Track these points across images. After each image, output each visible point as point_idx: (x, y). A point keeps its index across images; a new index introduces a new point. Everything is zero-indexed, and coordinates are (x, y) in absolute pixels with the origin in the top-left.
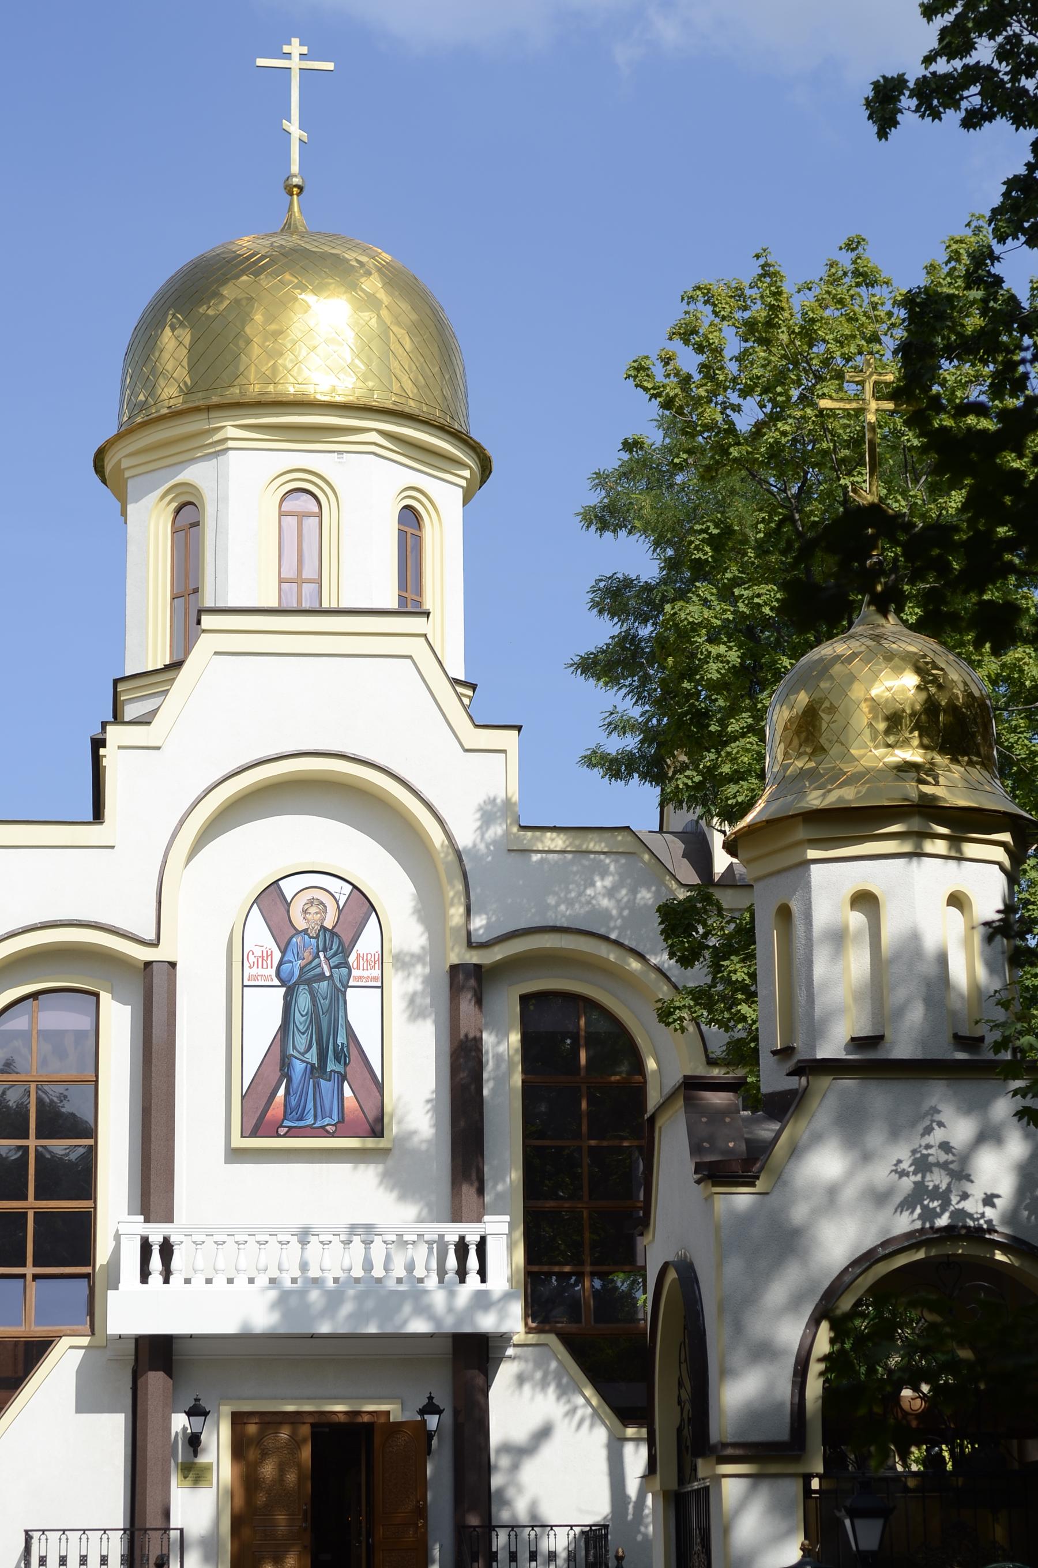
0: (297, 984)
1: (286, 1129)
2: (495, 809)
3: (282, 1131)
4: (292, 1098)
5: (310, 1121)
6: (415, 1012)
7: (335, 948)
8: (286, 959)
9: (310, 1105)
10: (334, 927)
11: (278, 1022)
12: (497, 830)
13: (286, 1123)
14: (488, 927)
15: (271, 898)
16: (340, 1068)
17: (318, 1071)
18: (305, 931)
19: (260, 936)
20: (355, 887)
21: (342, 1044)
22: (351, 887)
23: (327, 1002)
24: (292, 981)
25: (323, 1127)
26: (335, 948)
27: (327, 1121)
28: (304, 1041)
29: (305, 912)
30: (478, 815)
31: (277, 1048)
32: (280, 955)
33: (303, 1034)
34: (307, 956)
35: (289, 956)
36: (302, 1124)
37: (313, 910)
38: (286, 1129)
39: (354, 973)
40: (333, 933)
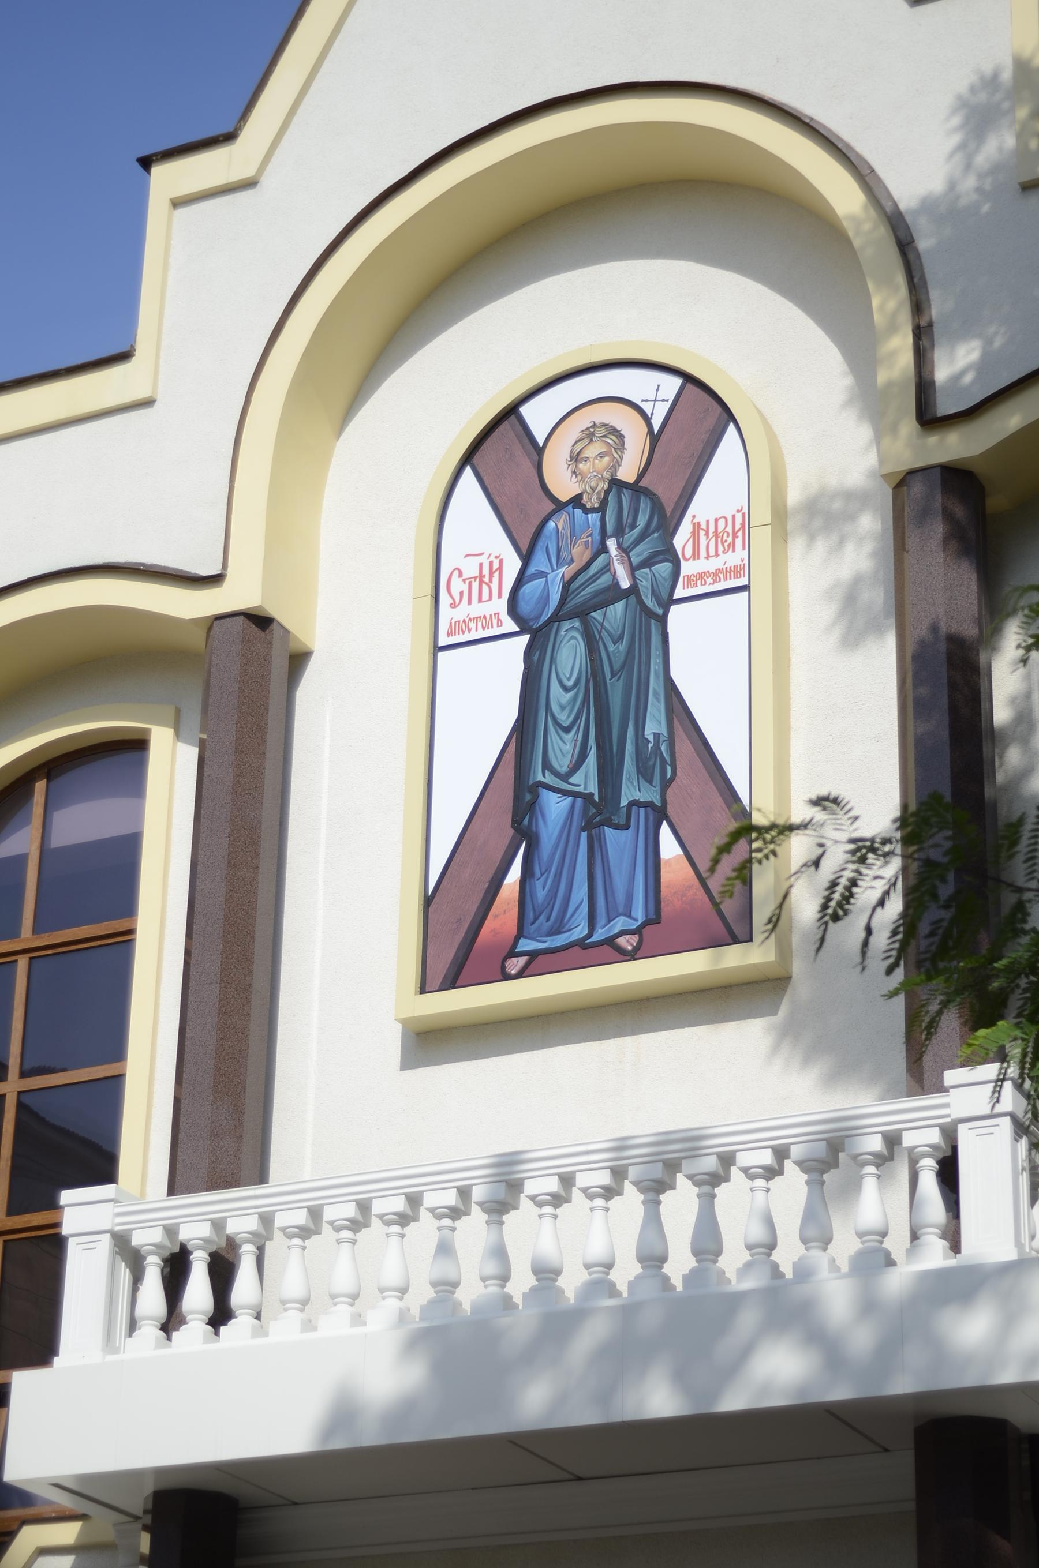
0: (557, 618)
1: (522, 961)
2: (998, 96)
3: (515, 965)
4: (539, 884)
5: (580, 931)
6: (853, 634)
7: (642, 521)
8: (531, 570)
9: (580, 893)
10: (641, 476)
11: (512, 714)
12: (1000, 143)
13: (525, 945)
14: (982, 367)
15: (500, 445)
16: (650, 794)
17: (598, 813)
18: (576, 501)
19: (477, 532)
20: (689, 379)
21: (657, 736)
22: (677, 382)
23: (623, 647)
24: (545, 617)
25: (610, 942)
26: (642, 521)
27: (620, 923)
28: (568, 748)
29: (576, 458)
30: (956, 120)
31: (508, 773)
32: (518, 564)
33: (567, 730)
34: (580, 553)
35: (540, 562)
36: (560, 940)
37: (593, 450)
38: (522, 961)
39: (687, 568)
40: (636, 489)
